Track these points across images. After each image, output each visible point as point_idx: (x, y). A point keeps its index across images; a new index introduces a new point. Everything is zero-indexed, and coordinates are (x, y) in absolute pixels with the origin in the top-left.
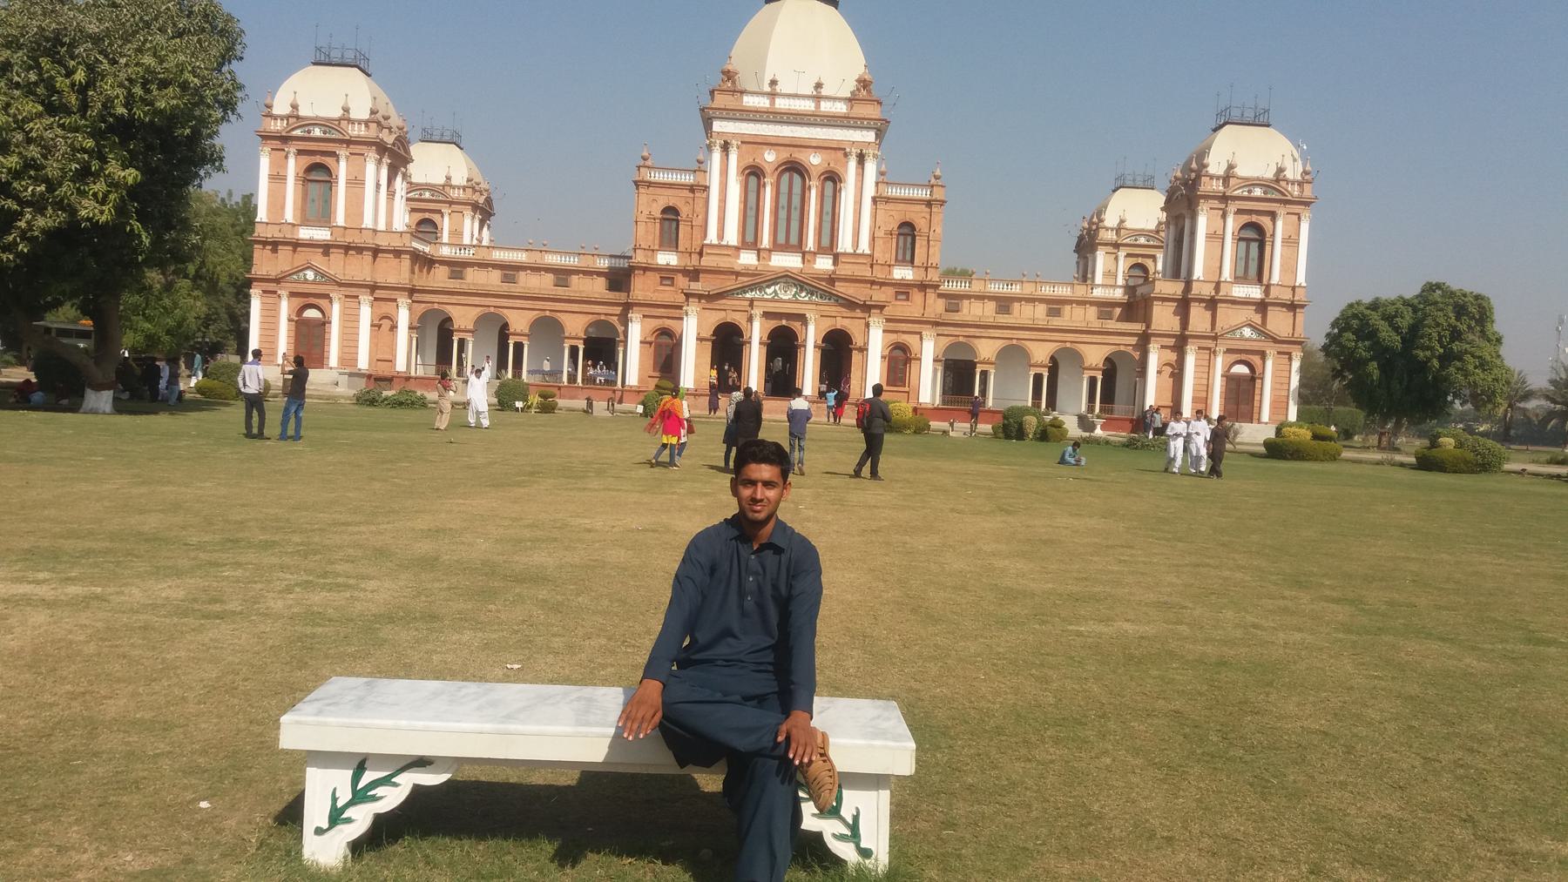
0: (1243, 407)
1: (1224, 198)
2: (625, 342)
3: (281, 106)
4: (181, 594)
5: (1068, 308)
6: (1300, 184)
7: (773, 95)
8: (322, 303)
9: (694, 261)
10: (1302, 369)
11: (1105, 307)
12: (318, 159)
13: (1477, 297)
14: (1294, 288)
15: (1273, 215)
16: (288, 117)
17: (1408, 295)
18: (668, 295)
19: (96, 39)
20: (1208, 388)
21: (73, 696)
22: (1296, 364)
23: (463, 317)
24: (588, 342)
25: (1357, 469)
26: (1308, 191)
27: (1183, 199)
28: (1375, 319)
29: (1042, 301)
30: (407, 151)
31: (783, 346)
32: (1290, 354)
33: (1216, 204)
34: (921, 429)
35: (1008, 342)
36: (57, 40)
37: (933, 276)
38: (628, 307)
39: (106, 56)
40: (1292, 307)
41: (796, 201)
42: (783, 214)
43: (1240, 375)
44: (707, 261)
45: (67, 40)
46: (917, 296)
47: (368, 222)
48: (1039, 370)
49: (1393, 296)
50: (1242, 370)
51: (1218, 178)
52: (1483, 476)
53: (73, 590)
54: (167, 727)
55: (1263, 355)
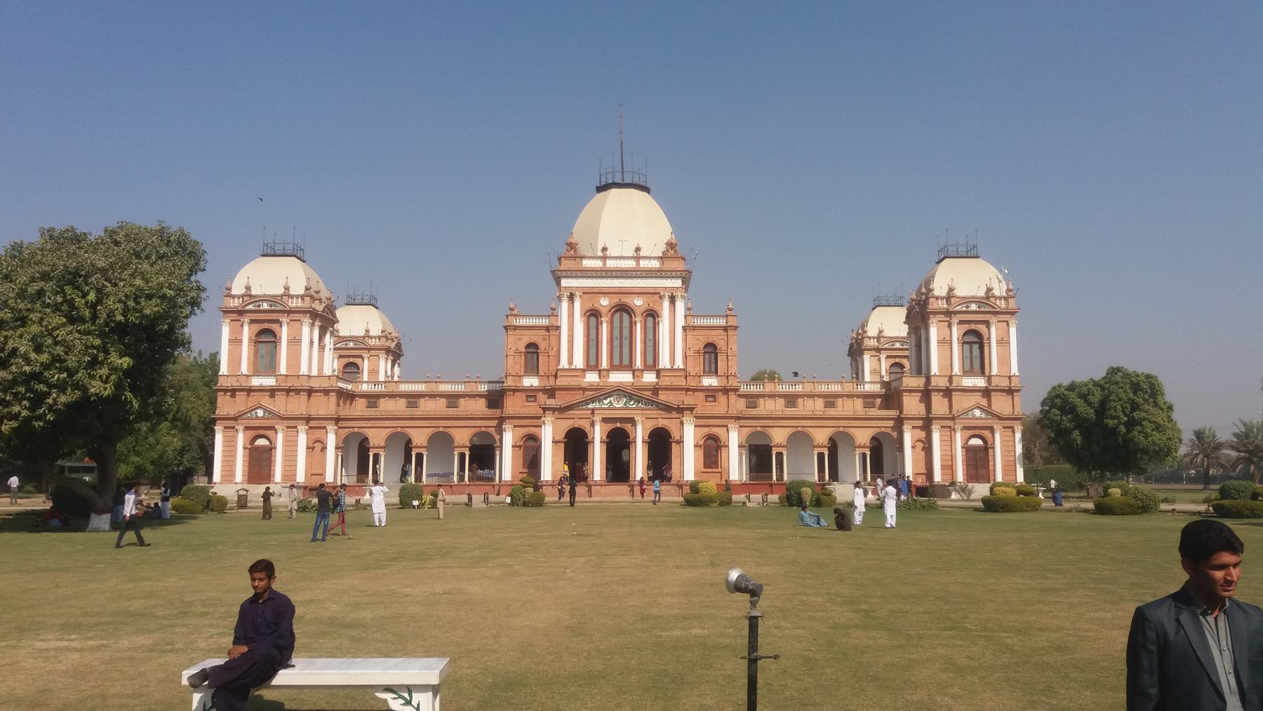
0: (982, 471)
1: (948, 313)
2: (501, 447)
3: (238, 289)
4: (150, 642)
5: (840, 400)
6: (1005, 299)
7: (604, 258)
8: (270, 433)
9: (551, 382)
10: (1024, 439)
11: (868, 398)
12: (266, 326)
13: (1148, 376)
14: (1010, 377)
15: (987, 323)
16: (243, 296)
17: (1097, 378)
18: (532, 409)
19: (103, 271)
20: (953, 457)
21: (94, 687)
22: (1018, 436)
23: (377, 437)
24: (473, 449)
25: (1054, 517)
26: (1012, 304)
27: (918, 316)
28: (1074, 398)
29: (819, 396)
30: (334, 315)
31: (618, 443)
32: (1012, 428)
33: (942, 317)
34: (727, 502)
35: (794, 430)
36: (76, 274)
37: (733, 382)
38: (502, 420)
39: (110, 281)
40: (1010, 392)
41: (626, 332)
42: (617, 343)
43: (973, 445)
44: (561, 382)
45: (83, 273)
46: (722, 398)
47: (304, 370)
48: (821, 450)
49: (1086, 379)
50: (976, 442)
51: (942, 298)
52: (1144, 516)
53: (90, 643)
54: (140, 696)
55: (992, 430)
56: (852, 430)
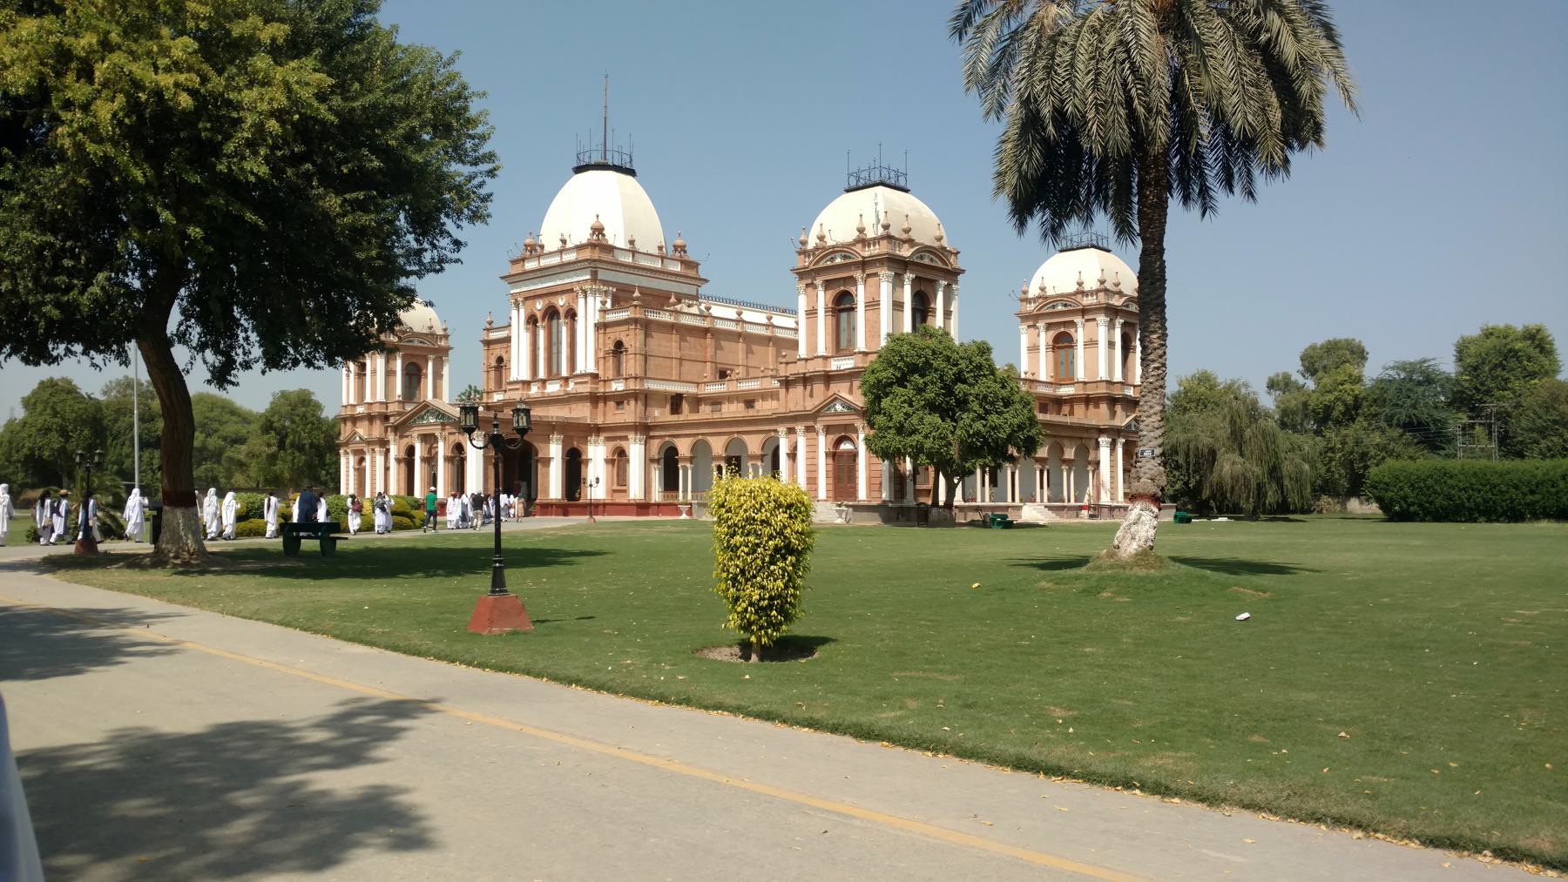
50: (846, 446)
56: (745, 437)
